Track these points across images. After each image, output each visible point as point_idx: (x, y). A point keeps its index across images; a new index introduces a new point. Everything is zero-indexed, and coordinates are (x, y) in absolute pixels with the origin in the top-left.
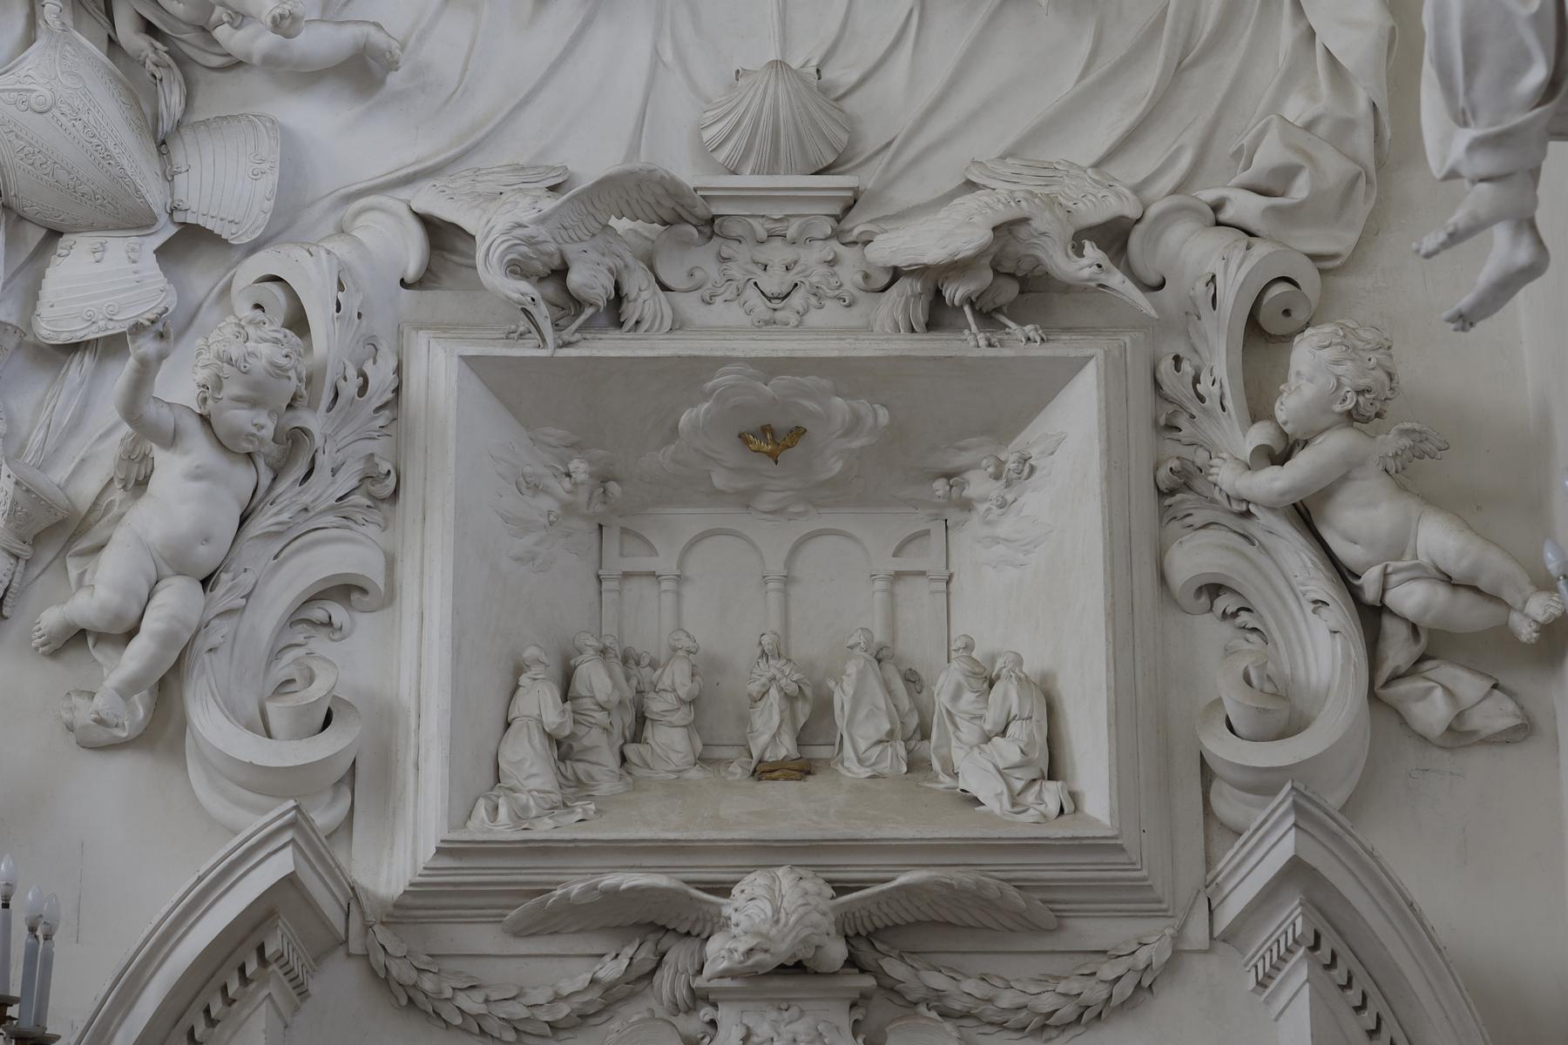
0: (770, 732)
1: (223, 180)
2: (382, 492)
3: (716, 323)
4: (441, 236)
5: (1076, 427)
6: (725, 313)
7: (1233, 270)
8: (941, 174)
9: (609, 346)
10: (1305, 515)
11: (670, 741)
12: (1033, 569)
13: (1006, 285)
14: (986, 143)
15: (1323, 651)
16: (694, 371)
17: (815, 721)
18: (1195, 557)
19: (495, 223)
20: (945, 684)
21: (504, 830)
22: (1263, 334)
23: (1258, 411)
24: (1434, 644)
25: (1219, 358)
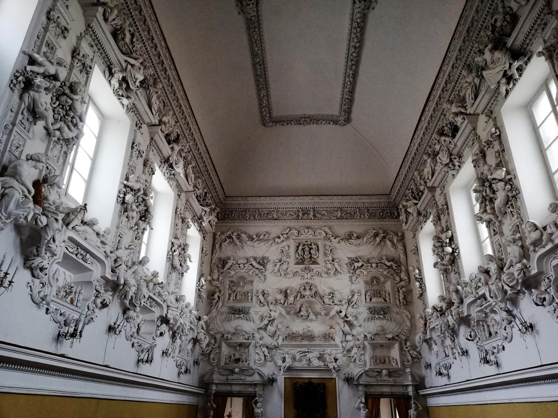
0: (383, 361)
1: (355, 332)
2: (364, 348)
3: (379, 340)
4: (365, 336)
5: (397, 346)
6: (379, 339)
7: (404, 338)
8: (388, 331)
9: (374, 342)
10: (408, 351)
11: (378, 361)
12: (395, 353)
13: (393, 338)
14: (391, 330)
15: (410, 358)
16: (378, 343)
17: (385, 360)
18: (403, 353)
19: (369, 336)
20: (391, 359)
21: (371, 367)
22: (406, 341)
23: (406, 345)
24: (415, 358)
25: (403, 343)
